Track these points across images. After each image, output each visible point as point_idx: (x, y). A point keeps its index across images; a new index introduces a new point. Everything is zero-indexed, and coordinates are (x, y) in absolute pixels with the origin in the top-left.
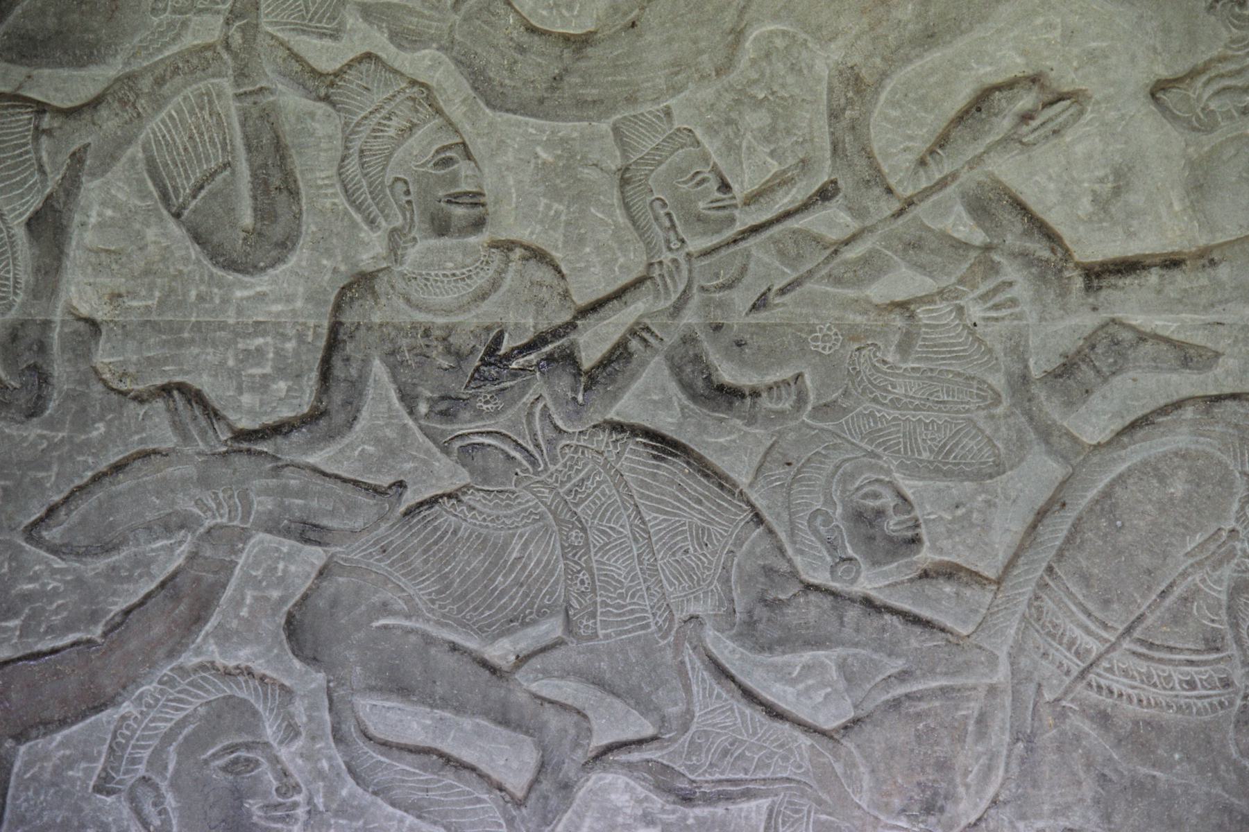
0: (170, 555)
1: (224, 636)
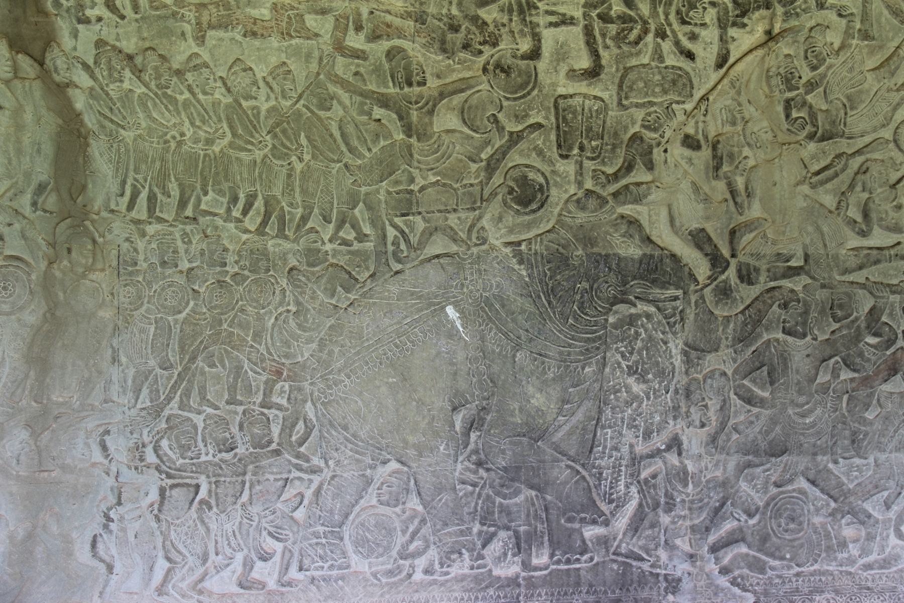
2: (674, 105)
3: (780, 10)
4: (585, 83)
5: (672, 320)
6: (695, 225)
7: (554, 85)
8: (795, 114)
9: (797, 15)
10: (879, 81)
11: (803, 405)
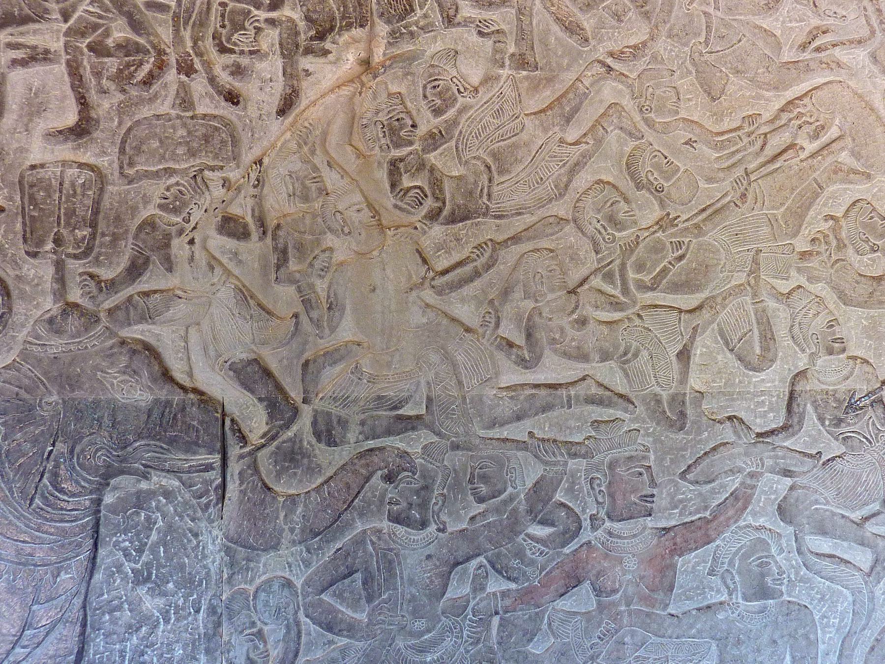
0: (734, 483)
1: (754, 514)
2: (207, 173)
3: (382, 29)
4: (70, 144)
5: (204, 500)
6: (241, 355)
7: (22, 150)
8: (407, 182)
9: (412, 34)
10: (545, 130)
11: (422, 634)
